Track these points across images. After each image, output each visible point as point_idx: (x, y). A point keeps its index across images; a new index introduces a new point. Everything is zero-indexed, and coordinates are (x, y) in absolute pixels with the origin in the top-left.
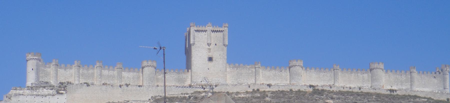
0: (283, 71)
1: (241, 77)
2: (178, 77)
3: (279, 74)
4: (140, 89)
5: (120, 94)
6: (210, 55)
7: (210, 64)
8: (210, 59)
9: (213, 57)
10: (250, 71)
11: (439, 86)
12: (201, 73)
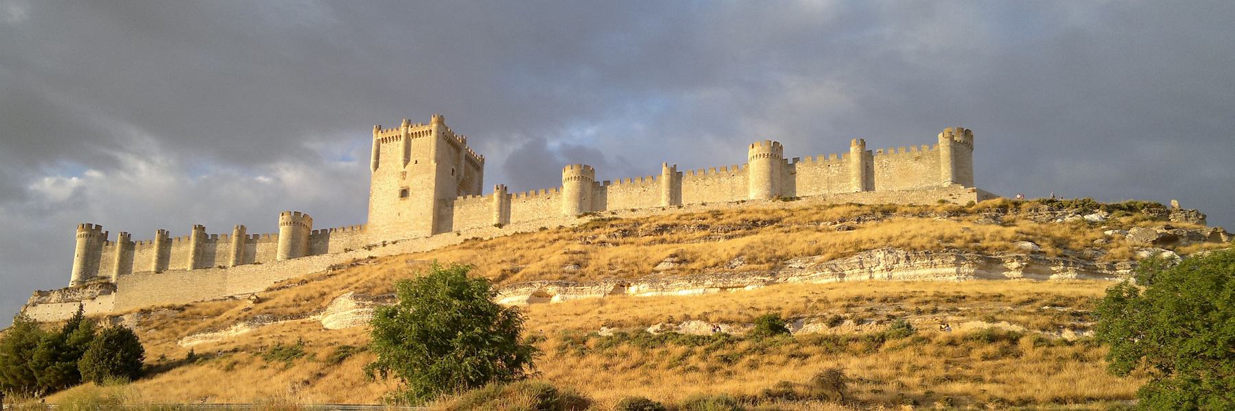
0: (553, 198)
1: (467, 223)
2: (351, 241)
3: (543, 206)
4: (256, 270)
5: (219, 283)
6: (405, 184)
7: (407, 202)
8: (404, 193)
9: (409, 189)
10: (486, 208)
11: (929, 178)
12: (383, 226)
